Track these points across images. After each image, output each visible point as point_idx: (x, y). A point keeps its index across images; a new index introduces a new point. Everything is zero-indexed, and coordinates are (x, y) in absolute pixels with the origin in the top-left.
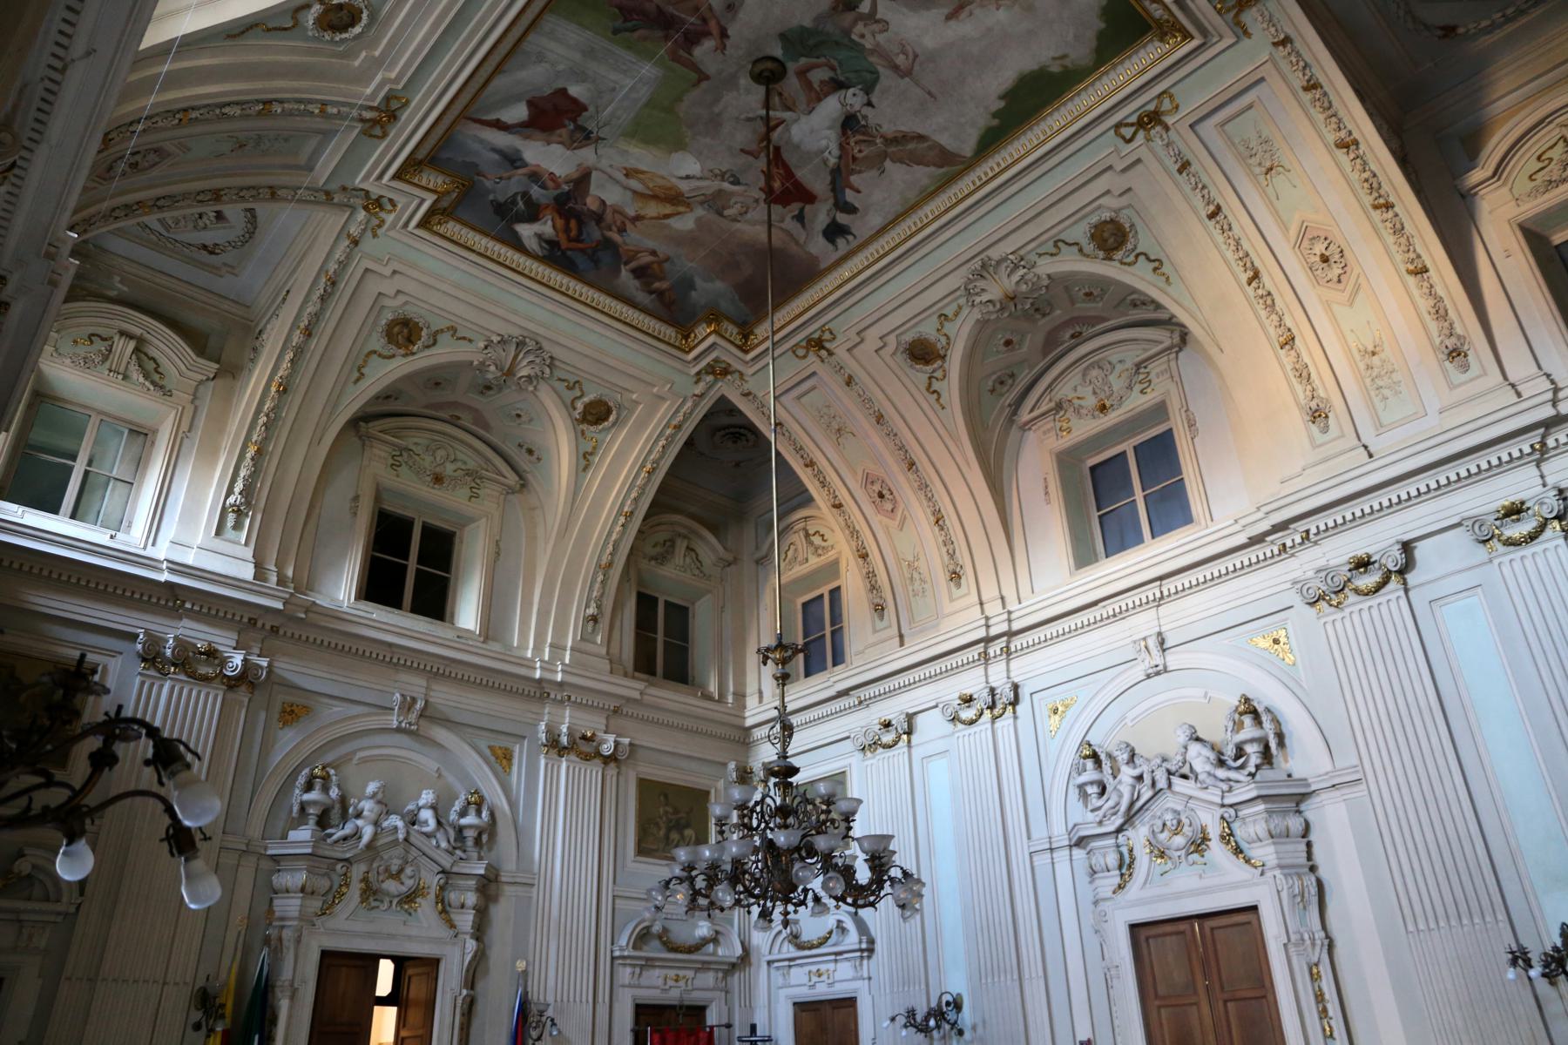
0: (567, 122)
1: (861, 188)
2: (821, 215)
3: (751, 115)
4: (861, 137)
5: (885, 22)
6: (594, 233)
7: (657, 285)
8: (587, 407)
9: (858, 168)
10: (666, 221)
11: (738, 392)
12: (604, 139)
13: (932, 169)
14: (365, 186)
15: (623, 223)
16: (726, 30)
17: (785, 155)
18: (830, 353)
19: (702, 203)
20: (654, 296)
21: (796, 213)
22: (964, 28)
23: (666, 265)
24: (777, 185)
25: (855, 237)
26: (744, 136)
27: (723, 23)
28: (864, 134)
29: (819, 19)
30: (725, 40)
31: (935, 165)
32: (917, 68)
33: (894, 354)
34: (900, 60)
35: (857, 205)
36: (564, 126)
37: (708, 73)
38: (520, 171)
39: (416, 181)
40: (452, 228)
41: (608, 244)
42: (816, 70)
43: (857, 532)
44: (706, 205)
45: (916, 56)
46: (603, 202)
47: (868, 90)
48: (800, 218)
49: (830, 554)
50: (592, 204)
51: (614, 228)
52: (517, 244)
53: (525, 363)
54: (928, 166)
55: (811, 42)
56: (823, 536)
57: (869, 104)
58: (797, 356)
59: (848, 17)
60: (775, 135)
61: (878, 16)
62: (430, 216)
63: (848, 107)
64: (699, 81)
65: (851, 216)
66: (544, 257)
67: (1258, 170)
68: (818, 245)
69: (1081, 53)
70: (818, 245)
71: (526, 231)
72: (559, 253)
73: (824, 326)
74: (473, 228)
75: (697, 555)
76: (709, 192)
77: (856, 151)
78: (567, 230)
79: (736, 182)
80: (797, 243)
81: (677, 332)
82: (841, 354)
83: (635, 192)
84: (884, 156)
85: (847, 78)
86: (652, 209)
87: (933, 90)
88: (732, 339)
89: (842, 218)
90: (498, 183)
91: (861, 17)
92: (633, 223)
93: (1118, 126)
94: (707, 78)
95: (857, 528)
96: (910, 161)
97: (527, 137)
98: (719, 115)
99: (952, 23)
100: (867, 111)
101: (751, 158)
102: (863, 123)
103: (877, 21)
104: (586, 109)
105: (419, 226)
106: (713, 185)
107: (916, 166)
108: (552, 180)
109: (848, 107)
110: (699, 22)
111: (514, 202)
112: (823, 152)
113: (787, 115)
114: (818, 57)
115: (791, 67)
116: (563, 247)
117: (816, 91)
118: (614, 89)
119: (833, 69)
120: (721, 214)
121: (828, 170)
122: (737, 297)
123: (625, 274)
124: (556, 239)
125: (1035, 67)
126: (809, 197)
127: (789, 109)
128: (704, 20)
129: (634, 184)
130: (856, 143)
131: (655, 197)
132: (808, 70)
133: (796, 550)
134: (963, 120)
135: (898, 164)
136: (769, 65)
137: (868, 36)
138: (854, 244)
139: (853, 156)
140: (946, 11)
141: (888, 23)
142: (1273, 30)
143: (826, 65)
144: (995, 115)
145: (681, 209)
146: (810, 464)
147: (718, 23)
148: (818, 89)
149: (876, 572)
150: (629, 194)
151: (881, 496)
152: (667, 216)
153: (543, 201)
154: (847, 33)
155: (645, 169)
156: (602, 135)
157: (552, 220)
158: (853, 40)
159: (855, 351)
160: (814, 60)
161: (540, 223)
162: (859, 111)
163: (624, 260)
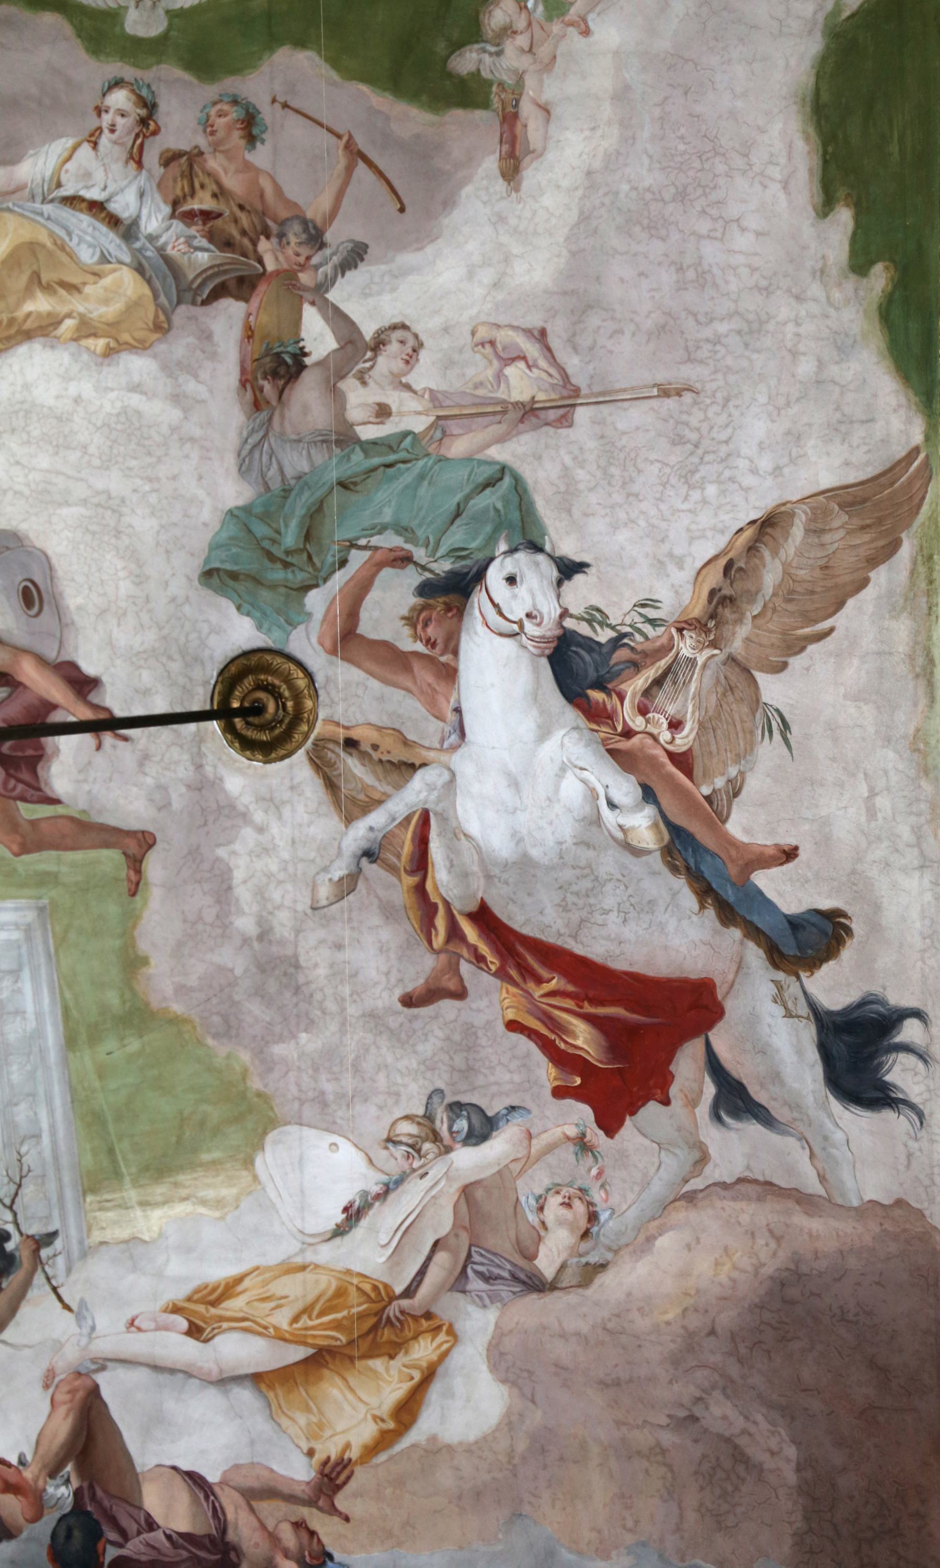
1: (788, 840)
3: (339, 871)
4: (641, 682)
5: (394, 327)
9: (720, 782)
10: (417, 1434)
12: (53, 1235)
13: (880, 577)
15: (299, 1525)
16: (73, 666)
19: (459, 1283)
21: (710, 1090)
25: (917, 1014)
27: (51, 654)
28: (636, 666)
30: (94, 698)
31: (874, 561)
32: (572, 363)
35: (825, 904)
42: (373, 595)
44: (475, 1284)
46: (194, 1479)
54: (863, 583)
55: (290, 538)
61: (368, 330)
63: (529, 627)
64: (136, 863)
83: (257, 1379)
85: (456, 553)
87: (661, 376)
92: (333, 1510)
96: (816, 622)
98: (264, 935)
99: (531, 175)
101: (447, 1007)
103: (378, 344)
107: (840, 620)
109: (529, 627)
112: (597, 820)
114: (343, 563)
117: (416, 654)
119: (403, 560)
121: (656, 861)
125: (814, 46)
127: (413, 768)
130: (643, 711)
132: (352, 616)
134: (806, 368)
135: (796, 662)
137: (394, 398)
139: (671, 755)
140: (490, 164)
141: (404, 327)
143: (380, 565)
147: (41, 660)
148: (419, 647)
150: (245, 1395)
156: (34, 1229)
158: (374, 443)
160: (339, 579)
162: (565, 614)
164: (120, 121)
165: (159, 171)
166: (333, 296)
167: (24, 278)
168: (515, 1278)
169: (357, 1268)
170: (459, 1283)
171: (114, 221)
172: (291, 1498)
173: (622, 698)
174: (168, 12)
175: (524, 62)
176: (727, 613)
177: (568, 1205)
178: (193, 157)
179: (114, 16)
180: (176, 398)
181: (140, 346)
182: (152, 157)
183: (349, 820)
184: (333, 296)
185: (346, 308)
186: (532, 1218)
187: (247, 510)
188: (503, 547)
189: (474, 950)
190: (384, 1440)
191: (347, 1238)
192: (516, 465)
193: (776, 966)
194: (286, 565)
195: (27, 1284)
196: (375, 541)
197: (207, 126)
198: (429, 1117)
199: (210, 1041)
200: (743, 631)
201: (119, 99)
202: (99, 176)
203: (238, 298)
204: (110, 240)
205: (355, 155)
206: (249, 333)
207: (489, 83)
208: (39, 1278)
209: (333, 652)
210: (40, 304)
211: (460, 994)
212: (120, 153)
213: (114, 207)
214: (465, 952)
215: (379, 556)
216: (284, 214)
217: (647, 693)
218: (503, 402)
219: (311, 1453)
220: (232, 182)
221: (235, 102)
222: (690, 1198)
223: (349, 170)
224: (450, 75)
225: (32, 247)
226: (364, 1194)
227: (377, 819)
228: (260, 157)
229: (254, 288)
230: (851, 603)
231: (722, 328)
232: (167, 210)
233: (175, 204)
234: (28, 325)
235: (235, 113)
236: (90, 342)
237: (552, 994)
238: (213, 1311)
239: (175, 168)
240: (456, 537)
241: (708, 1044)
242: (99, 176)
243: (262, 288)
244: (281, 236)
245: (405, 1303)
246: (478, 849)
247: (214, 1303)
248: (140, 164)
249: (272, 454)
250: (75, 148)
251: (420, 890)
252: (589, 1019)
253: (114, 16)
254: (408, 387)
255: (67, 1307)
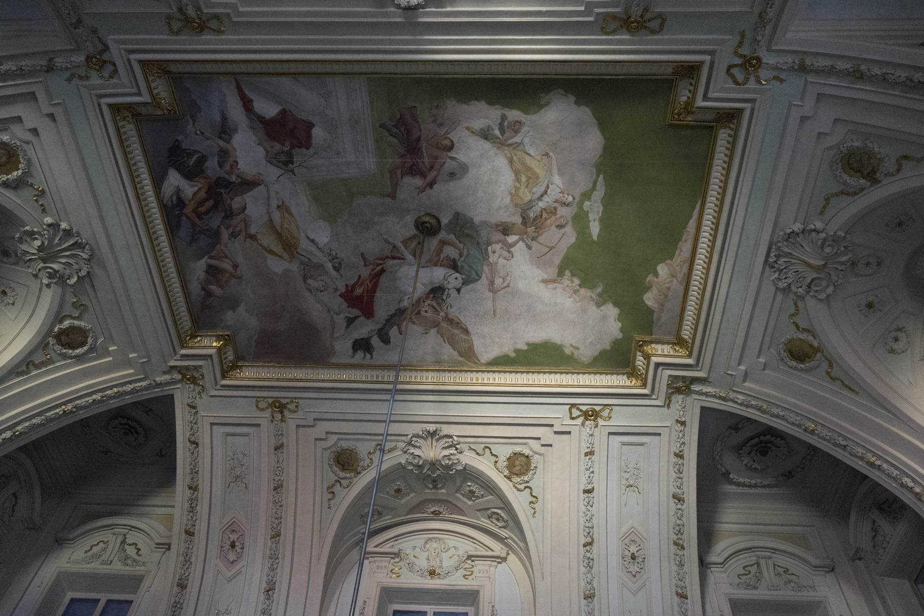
0: (287, 143)
2: (364, 329)
3: (390, 239)
4: (435, 305)
5: (513, 255)
6: (215, 221)
7: (213, 288)
8: (72, 329)
9: (415, 320)
11: (186, 401)
13: (456, 353)
14: (112, 46)
15: (240, 231)
17: (383, 280)
18: (283, 420)
19: (302, 263)
20: (203, 293)
21: (352, 316)
22: (546, 293)
23: (234, 281)
24: (359, 291)
25: (372, 357)
26: (373, 248)
27: (438, 178)
28: (438, 304)
29: (484, 223)
30: (428, 188)
32: (502, 292)
33: (326, 449)
34: (498, 282)
35: (392, 340)
36: (283, 145)
37: (397, 195)
38: (221, 143)
39: (150, 79)
40: (130, 130)
41: (215, 236)
42: (452, 248)
43: (191, 563)
44: (302, 267)
45: (508, 286)
46: (245, 208)
47: (465, 283)
48: (350, 321)
49: (138, 568)
50: (236, 203)
51: (231, 230)
52: (158, 183)
53: (63, 261)
54: (455, 350)
55: (466, 231)
56: (139, 550)
57: (458, 290)
58: (257, 406)
59: (500, 236)
60: (391, 262)
61: (512, 249)
62: (125, 108)
64: (389, 196)
65: (382, 344)
66: (165, 206)
67: (624, 482)
68: (343, 346)
69: (586, 353)
70: (343, 346)
71: (174, 179)
72: (177, 212)
73: (296, 398)
74: (143, 144)
75: (16, 504)
76: (315, 260)
77: (424, 309)
78: (201, 203)
79: (337, 269)
80: (332, 334)
81: (190, 329)
82: (291, 424)
84: (436, 324)
85: (463, 266)
86: (268, 240)
87: (498, 311)
88: (224, 361)
89: (375, 341)
90: (197, 134)
91: (504, 242)
92: (246, 238)
93: (573, 405)
94: (394, 198)
95: (193, 560)
97: (252, 128)
99: (542, 285)
100: (454, 293)
101: (362, 263)
102: (444, 297)
103: (509, 252)
104: (308, 149)
105: (110, 106)
106: (319, 257)
107: (447, 345)
108: (231, 166)
110: (428, 166)
111: (190, 154)
113: (409, 257)
114: (460, 242)
115: (443, 235)
116: (184, 211)
118: (339, 153)
119: (461, 256)
120: (305, 279)
122: (255, 338)
123: (202, 264)
124: (187, 203)
125: (559, 342)
126: (369, 313)
127: (415, 256)
128: (432, 168)
129: (277, 216)
130: (429, 305)
131: (279, 235)
133: (104, 549)
135: (439, 336)
136: (433, 221)
137: (497, 255)
138: (368, 361)
140: (546, 277)
141: (512, 257)
142: (682, 413)
143: (460, 250)
144: (516, 351)
145: (285, 256)
146: (193, 488)
147: (436, 177)
148: (442, 258)
149: (184, 605)
151: (233, 545)
152: (271, 252)
153: (209, 173)
154: (489, 244)
155: (295, 216)
156: (296, 171)
157: (200, 189)
159: (301, 430)
161: (190, 182)
162: (449, 289)
163: (212, 255)
164: (565, 198)
165: (553, 206)
166: (521, 242)
167: (530, 176)
168: (305, 275)
169: (301, 241)
170: (302, 263)
171: (542, 196)
172: (246, 230)
173: (432, 301)
174: (588, 211)
175: (565, 285)
176: (449, 323)
177: (323, 286)
178: (555, 214)
179: (589, 199)
180: (500, 208)
181: (512, 201)
182: (556, 205)
183: (402, 242)
184: (521, 242)
185: (518, 245)
186: (319, 278)
187: (473, 222)
188: (464, 277)
189: (375, 269)
190: (265, 248)
191: (307, 240)
192: (481, 280)
193: (378, 330)
194: (460, 231)
195: (282, 169)
196: (465, 250)
197: (562, 217)
198: (337, 258)
199: (347, 211)
200: (445, 326)
201: (570, 199)
202: (553, 193)
203: (522, 222)
204: (538, 195)
205: (551, 248)
206: (513, 224)
207: (562, 277)
208: (284, 172)
209: (440, 240)
210: (524, 179)
211: (365, 265)
212: (558, 198)
213: (545, 196)
214: (374, 267)
215: (462, 250)
216: (540, 233)
217: (432, 306)
218: (495, 276)
219: (257, 233)
220: (548, 222)
221: (566, 224)
222: (329, 311)
223: (548, 247)
224: (565, 269)
225: (538, 178)
226: (318, 243)
227: (403, 248)
228: (553, 227)
229: (524, 225)
230: (451, 347)
231: (506, 323)
232: (544, 207)
233: (545, 209)
234: (519, 176)
235: (564, 223)
236: (514, 190)
237: (368, 285)
238: (284, 210)
239: (553, 209)
240: (466, 267)
241: (359, 316)
242: (553, 193)
243: (524, 227)
244: (535, 232)
245: (295, 252)
246: (397, 270)
247: (286, 211)
248: (555, 202)
249: (486, 228)
250: (560, 188)
251: (387, 258)
252: (363, 293)
253: (589, 199)
254: (499, 257)
255: (278, 178)
